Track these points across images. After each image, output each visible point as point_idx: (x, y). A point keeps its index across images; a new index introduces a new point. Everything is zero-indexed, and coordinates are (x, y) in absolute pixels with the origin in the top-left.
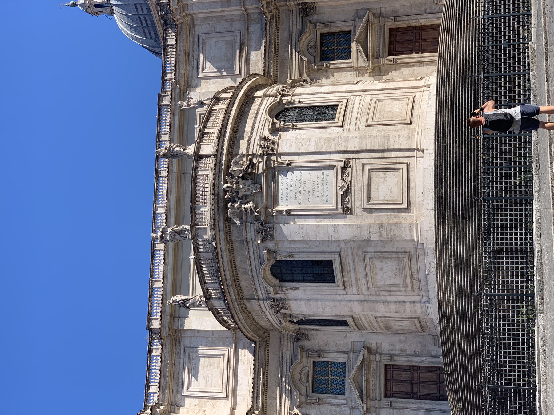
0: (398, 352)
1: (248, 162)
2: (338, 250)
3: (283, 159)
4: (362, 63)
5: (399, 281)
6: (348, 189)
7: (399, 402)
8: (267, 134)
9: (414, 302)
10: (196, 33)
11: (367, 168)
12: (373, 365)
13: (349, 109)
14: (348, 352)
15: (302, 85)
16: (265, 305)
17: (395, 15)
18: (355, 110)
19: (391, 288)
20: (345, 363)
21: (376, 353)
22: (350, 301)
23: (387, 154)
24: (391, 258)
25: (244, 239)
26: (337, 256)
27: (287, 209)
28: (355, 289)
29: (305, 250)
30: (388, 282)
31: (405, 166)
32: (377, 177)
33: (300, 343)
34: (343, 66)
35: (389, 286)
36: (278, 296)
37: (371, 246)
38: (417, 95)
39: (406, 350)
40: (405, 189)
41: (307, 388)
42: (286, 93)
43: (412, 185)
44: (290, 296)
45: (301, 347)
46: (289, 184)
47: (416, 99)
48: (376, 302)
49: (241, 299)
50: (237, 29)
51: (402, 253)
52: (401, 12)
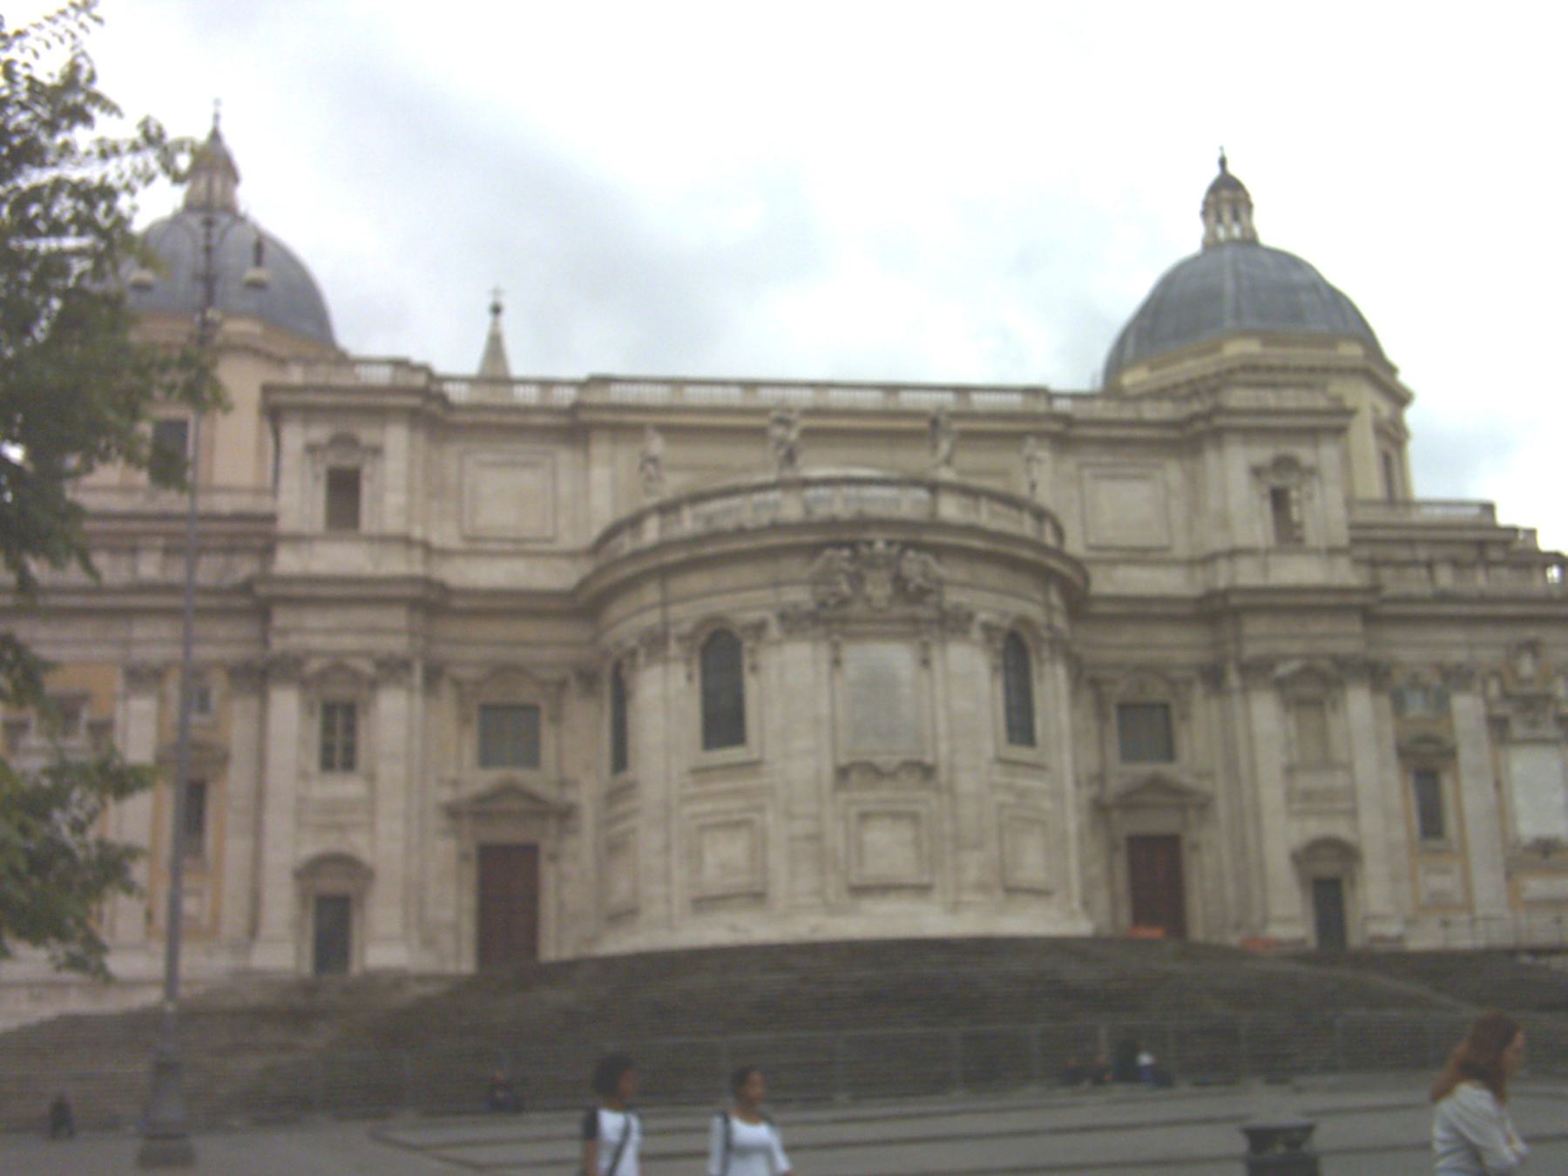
3: (935, 653)
4: (1115, 785)
7: (471, 874)
8: (983, 616)
16: (652, 619)
19: (695, 857)
26: (755, 756)
31: (925, 879)
32: (905, 832)
45: (562, 685)
49: (666, 573)
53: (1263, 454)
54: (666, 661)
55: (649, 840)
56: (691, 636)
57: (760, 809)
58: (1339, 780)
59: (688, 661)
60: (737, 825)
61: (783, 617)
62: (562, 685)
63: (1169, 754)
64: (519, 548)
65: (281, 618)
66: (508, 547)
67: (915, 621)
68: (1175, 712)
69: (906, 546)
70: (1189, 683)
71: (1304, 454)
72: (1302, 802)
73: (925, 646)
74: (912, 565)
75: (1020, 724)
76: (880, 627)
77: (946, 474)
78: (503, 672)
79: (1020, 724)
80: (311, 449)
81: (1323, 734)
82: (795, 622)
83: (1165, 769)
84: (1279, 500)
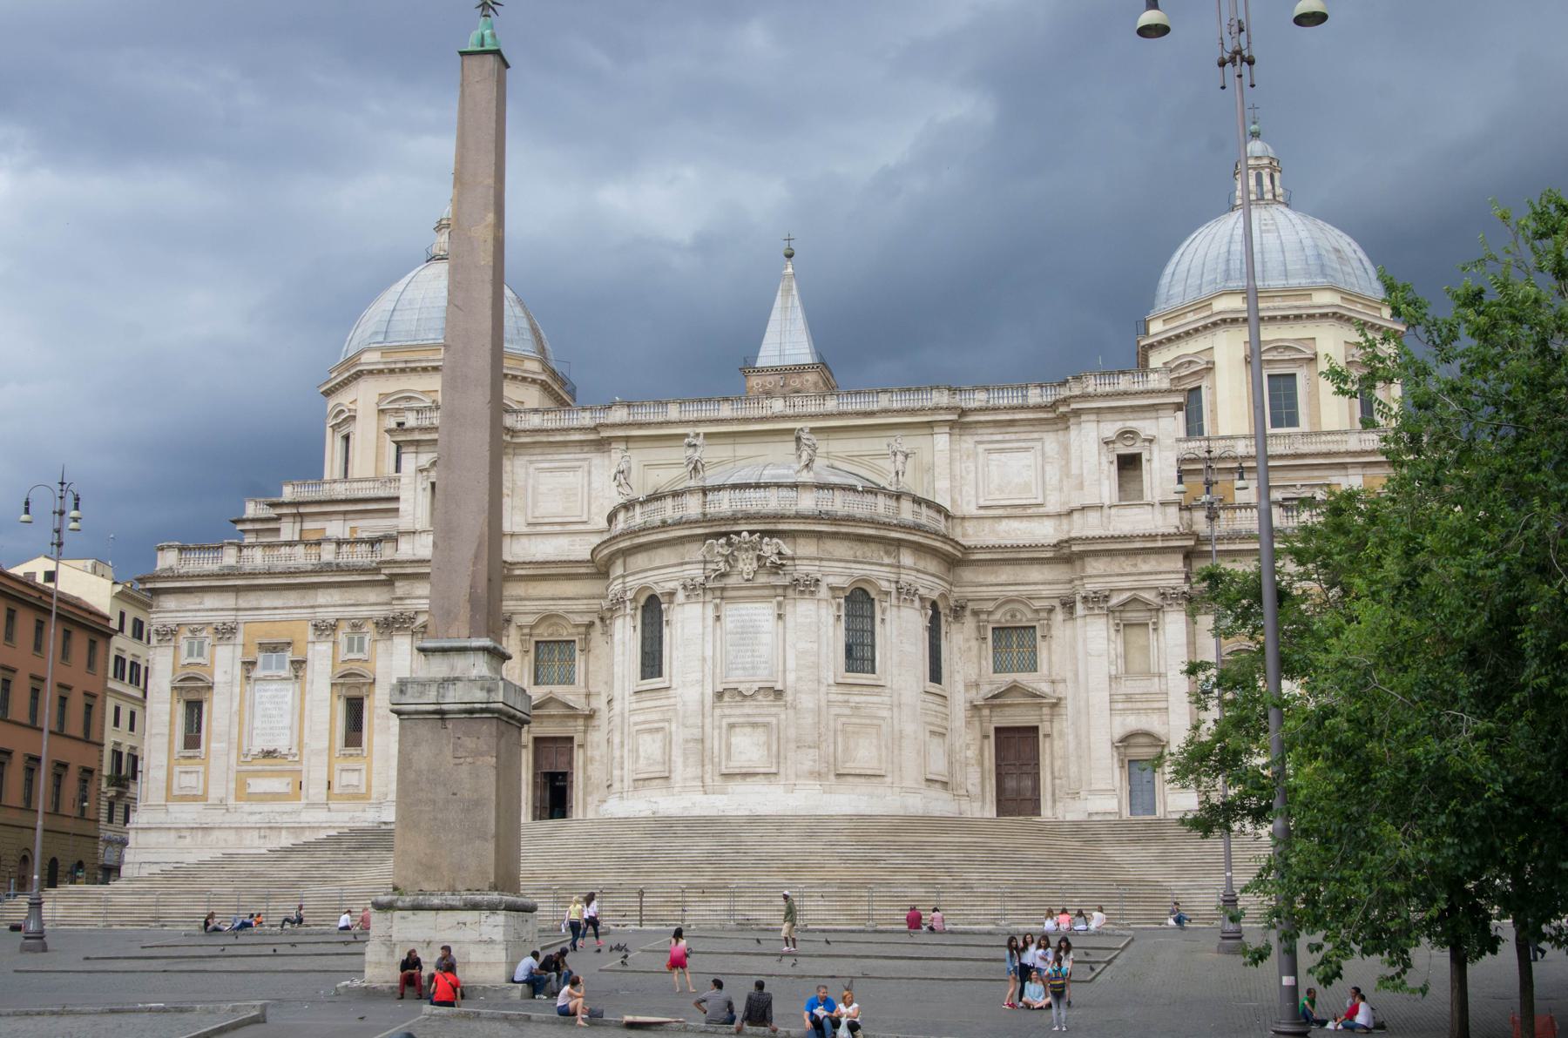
0: (589, 753)
1: (779, 562)
2: (674, 686)
4: (987, 690)
5: (642, 761)
6: (745, 696)
8: (831, 580)
9: (622, 781)
10: (1045, 435)
11: (774, 721)
12: (571, 723)
13: (865, 689)
14: (587, 686)
15: (926, 614)
17: (1055, 734)
18: (863, 698)
20: (573, 683)
21: (586, 726)
22: (623, 698)
23: (792, 746)
24: (664, 753)
25: (687, 560)
26: (666, 685)
27: (723, 617)
28: (635, 706)
29: (674, 642)
30: (641, 749)
31: (774, 770)
32: (760, 736)
33: (597, 622)
34: (984, 662)
35: (637, 750)
36: (628, 603)
37: (678, 727)
38: (888, 780)
39: (592, 764)
40: (744, 771)
41: (542, 635)
42: (903, 597)
43: (748, 780)
44: (628, 618)
45: (591, 624)
46: (754, 617)
47: (879, 779)
48: (622, 733)
49: (626, 553)
50: (1048, 498)
51: (670, 767)
52: (1057, 744)
53: (1111, 428)
54: (625, 616)
55: (616, 739)
56: (634, 600)
57: (669, 721)
58: (1155, 685)
59: (633, 617)
60: (657, 730)
61: (685, 587)
62: (591, 624)
63: (1033, 667)
64: (564, 528)
65: (401, 588)
66: (558, 528)
67: (775, 587)
68: (1039, 634)
69: (764, 533)
70: (1051, 610)
71: (1145, 426)
72: (1122, 702)
73: (780, 604)
74: (769, 548)
75: (859, 655)
76: (752, 591)
77: (806, 477)
78: (547, 618)
79: (859, 655)
80: (421, 471)
81: (1147, 648)
82: (694, 589)
83: (1024, 678)
84: (1129, 464)
